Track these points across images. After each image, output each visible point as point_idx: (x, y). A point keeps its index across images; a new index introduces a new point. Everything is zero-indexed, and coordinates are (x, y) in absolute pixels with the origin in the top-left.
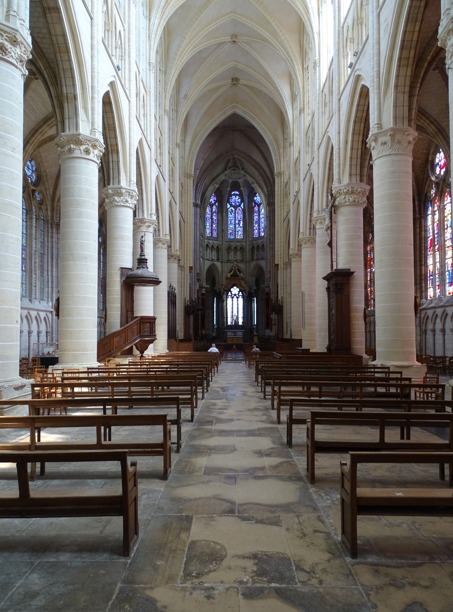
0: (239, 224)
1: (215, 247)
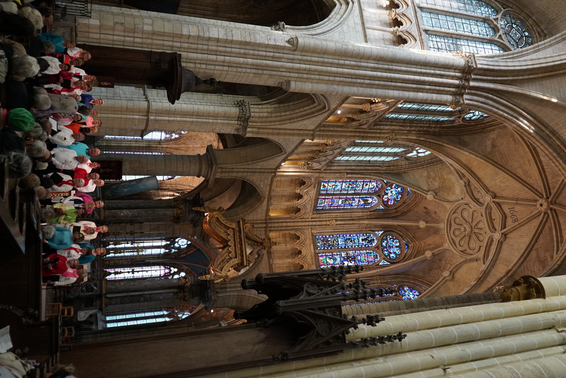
0: (348, 258)
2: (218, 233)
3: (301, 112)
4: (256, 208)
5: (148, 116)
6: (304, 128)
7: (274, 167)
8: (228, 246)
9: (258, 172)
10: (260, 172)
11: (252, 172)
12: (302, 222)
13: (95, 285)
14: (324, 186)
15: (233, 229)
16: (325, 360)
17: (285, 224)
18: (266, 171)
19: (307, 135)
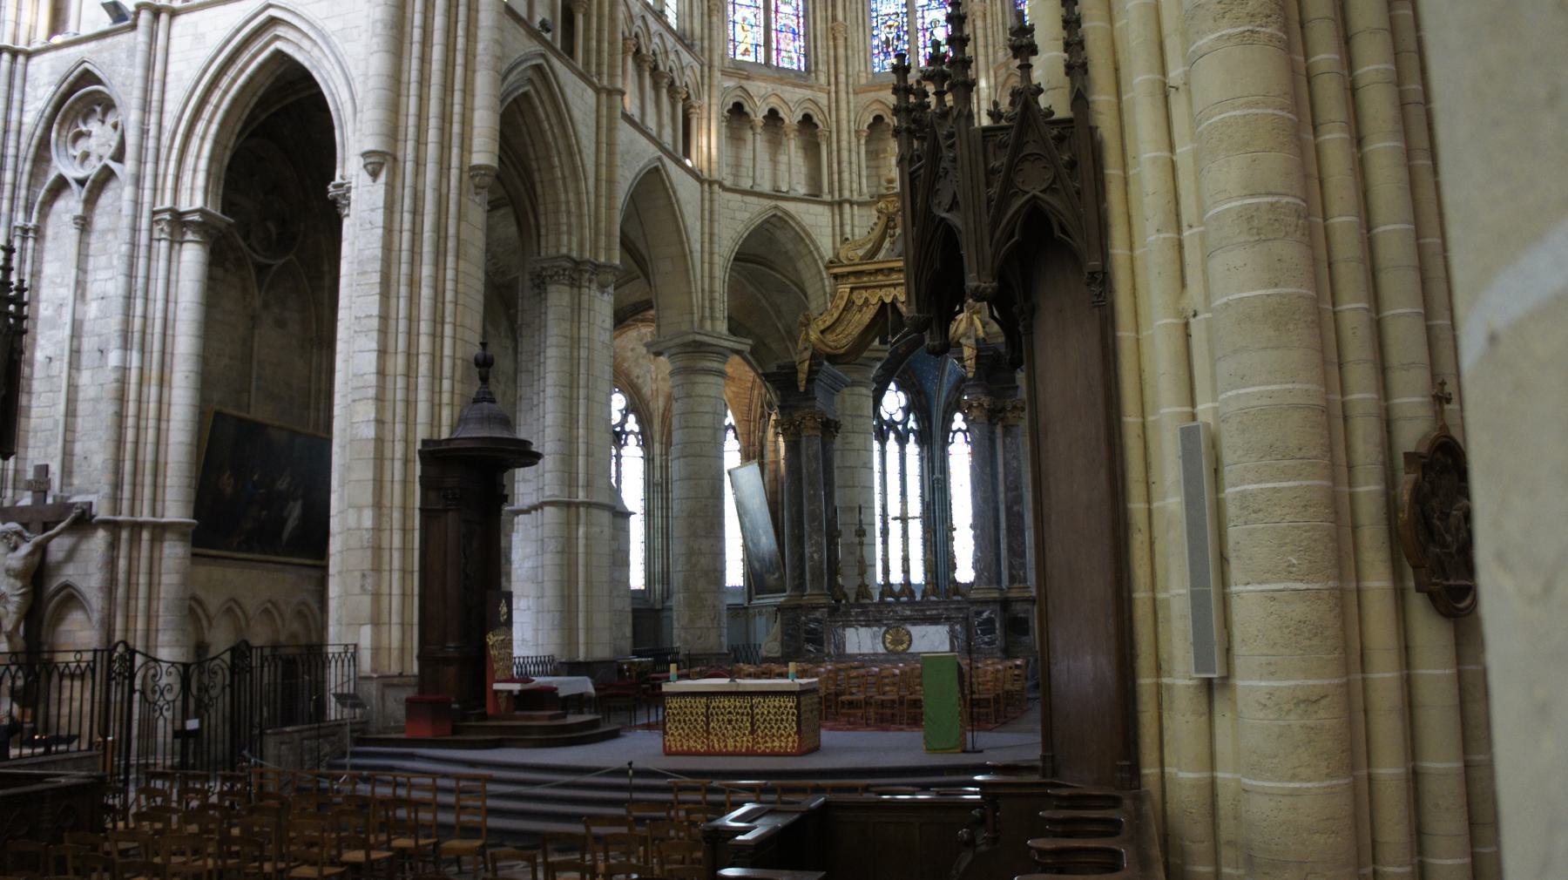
1: (791, 118)
2: (861, 328)
3: (551, 126)
4: (804, 229)
5: (578, 505)
6: (594, 116)
7: (697, 184)
8: (893, 304)
9: (711, 227)
10: (711, 221)
11: (711, 242)
12: (838, 109)
13: (979, 614)
14: (746, 52)
15: (852, 289)
16: (1112, 171)
17: (845, 154)
18: (707, 206)
19: (611, 108)
